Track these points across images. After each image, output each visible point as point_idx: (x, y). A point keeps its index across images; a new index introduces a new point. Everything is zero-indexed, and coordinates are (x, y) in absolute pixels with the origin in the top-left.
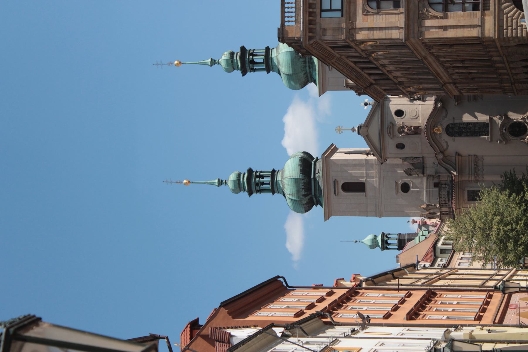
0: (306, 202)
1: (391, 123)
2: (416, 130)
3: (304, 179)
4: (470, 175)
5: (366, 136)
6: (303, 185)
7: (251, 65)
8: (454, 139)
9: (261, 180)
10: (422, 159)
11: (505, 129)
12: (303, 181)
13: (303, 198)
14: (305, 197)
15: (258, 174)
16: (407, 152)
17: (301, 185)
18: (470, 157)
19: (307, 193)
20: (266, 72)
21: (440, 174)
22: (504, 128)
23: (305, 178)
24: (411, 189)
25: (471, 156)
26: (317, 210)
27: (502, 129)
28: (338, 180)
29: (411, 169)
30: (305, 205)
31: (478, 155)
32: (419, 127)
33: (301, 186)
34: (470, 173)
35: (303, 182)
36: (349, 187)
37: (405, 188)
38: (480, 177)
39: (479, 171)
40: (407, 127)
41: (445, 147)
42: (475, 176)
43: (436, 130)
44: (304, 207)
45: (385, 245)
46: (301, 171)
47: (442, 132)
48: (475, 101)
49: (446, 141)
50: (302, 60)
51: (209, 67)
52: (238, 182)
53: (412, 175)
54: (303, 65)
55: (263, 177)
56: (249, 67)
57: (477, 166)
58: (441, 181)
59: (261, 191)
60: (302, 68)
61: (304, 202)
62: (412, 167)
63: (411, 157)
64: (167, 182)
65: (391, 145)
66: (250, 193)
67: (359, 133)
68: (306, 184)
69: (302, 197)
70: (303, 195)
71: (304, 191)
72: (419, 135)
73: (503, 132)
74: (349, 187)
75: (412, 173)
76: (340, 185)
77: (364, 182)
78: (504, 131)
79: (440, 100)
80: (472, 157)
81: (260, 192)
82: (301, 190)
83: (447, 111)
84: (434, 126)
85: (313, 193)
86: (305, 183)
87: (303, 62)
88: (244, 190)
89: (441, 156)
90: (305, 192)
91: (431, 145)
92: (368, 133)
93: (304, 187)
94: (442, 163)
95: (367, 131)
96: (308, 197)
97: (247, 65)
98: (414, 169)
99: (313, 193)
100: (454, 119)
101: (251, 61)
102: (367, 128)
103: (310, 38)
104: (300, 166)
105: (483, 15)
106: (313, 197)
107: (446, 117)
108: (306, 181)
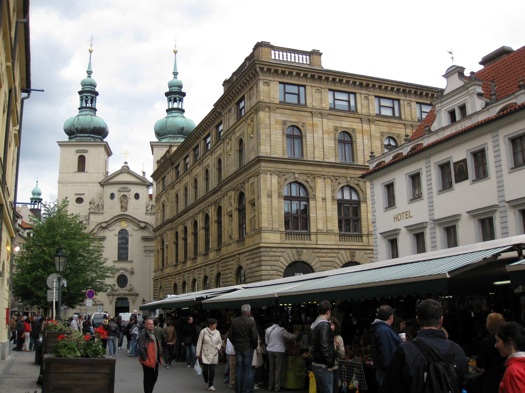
1: (130, 190)
2: (124, 207)
7: (173, 98)
9: (90, 100)
12: (88, 128)
15: (94, 99)
16: (107, 201)
17: (85, 126)
20: (167, 108)
22: (123, 271)
24: (78, 205)
26: (65, 138)
29: (94, 204)
30: (69, 129)
32: (127, 210)
36: (82, 160)
37: (79, 200)
40: (127, 201)
41: (110, 229)
44: (68, 129)
45: (34, 201)
46: (95, 127)
50: (176, 132)
51: (172, 71)
52: (90, 84)
55: (92, 103)
59: (82, 99)
61: (72, 128)
62: (96, 204)
64: (92, 37)
65: (114, 189)
66: (80, 93)
67: (123, 167)
69: (76, 126)
70: (78, 128)
71: (81, 128)
72: (120, 210)
74: (82, 160)
78: (121, 271)
79: (146, 225)
85: (78, 135)
86: (86, 129)
87: (175, 133)
88: (82, 89)
89: (104, 225)
91: (113, 218)
96: (75, 131)
97: (173, 96)
99: (78, 135)
103: (262, 69)
105: (281, 232)
106: (75, 135)
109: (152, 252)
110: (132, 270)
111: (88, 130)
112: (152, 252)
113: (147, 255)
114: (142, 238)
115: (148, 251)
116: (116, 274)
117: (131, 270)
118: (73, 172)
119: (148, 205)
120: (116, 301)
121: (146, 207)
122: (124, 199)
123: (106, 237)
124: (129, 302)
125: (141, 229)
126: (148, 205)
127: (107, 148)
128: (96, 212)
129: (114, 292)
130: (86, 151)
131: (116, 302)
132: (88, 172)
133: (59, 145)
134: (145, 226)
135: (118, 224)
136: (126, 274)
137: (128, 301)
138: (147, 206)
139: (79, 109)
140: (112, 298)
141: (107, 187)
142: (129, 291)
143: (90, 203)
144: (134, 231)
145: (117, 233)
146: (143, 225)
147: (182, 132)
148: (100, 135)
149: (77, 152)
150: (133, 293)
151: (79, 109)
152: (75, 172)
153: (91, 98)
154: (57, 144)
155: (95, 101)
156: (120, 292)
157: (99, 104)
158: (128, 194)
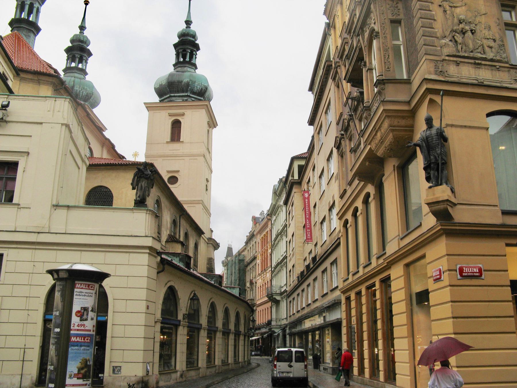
15: (194, 53)
26: (156, 99)
36: (176, 125)
74: (176, 125)
76: (180, 118)
127: (209, 111)
130: (183, 115)
132: (184, 141)
133: (146, 107)
139: (174, 65)
148: (201, 97)
149: (170, 115)
151: (174, 65)
152: (167, 142)
153: (190, 51)
154: (144, 106)
155: (195, 56)
157: (200, 58)
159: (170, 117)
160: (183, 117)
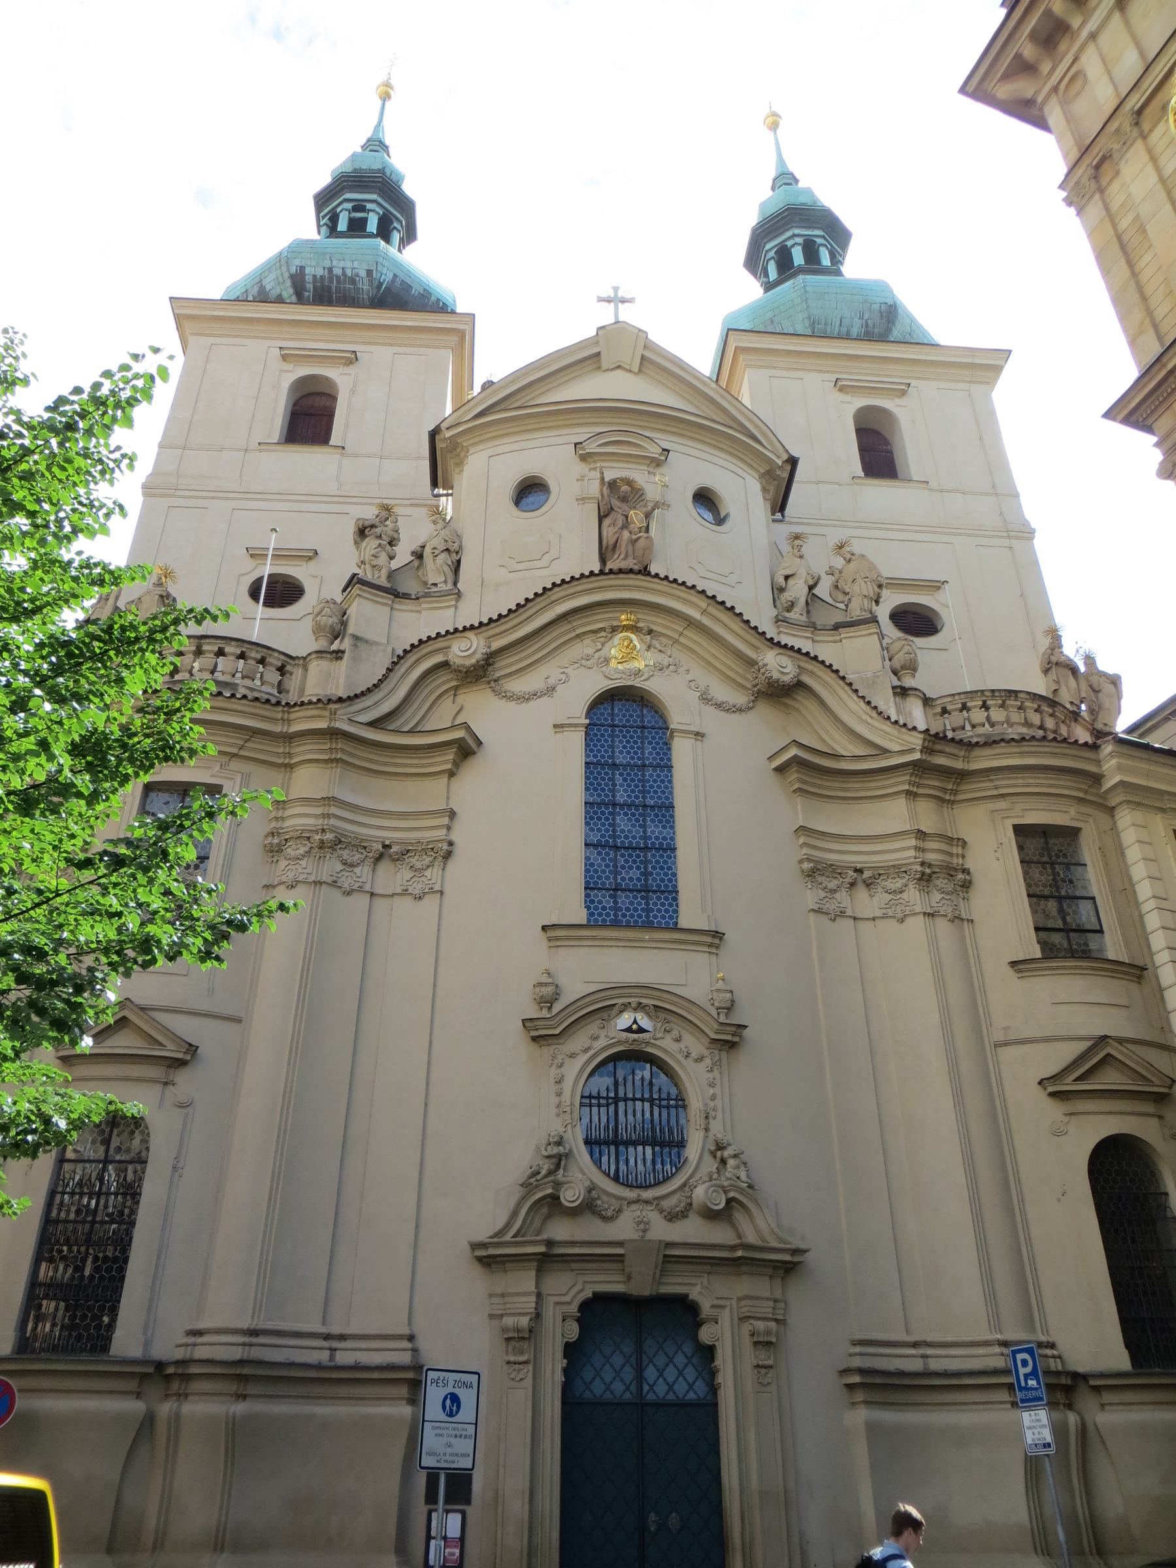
0: (268, 288)
3: (371, 282)
4: (319, 811)
5: (598, 354)
6: (344, 273)
7: (799, 240)
8: (570, 725)
10: (442, 587)
11: (641, 1030)
12: (363, 274)
13: (288, 270)
14: (292, 277)
17: (348, 264)
18: (446, 821)
19: (310, 286)
21: (346, 656)
23: (376, 284)
25: (449, 828)
27: (640, 1007)
28: (352, 366)
30: (256, 289)
31: (452, 865)
33: (342, 264)
34: (333, 810)
35: (357, 275)
38: (303, 863)
39: (339, 867)
40: (648, 516)
41: (517, 685)
42: (316, 832)
43: (631, 641)
47: (616, 671)
48: (806, 866)
49: (558, 688)
53: (356, 543)
54: (837, 328)
56: (794, 235)
57: (379, 858)
58: (306, 669)
60: (825, 324)
62: (403, 556)
63: (460, 547)
68: (347, 286)
69: (297, 262)
70: (302, 268)
71: (320, 272)
73: (621, 1012)
75: (370, 544)
77: (331, 443)
78: (625, 1020)
79: (806, 679)
80: (444, 831)
81: (328, 223)
82: (327, 264)
83: (740, 710)
84: (650, 632)
86: (353, 281)
87: (848, 333)
89: (465, 651)
90: (315, 276)
92: (608, 370)
93: (338, 277)
94: (418, 662)
95: (619, 367)
97: (797, 231)
98: (391, 558)
100: (699, 735)
101: (815, 242)
102: (636, 369)
104: (422, 292)
107: (706, 699)
108: (361, 286)
109: (868, 884)
110: (730, 1008)
111: (364, 286)
112: (868, 884)
113: (831, 906)
114: (780, 770)
115: (834, 870)
116: (579, 1041)
117: (714, 1013)
118: (253, 444)
119: (787, 578)
120: (573, 1331)
121: (778, 590)
122: (624, 499)
123: (480, 743)
124: (708, 1352)
125: (764, 709)
126: (787, 578)
128: (401, 590)
129: (561, 1230)
131: (570, 1350)
134: (799, 685)
135: (586, 647)
136: (666, 1046)
137: (706, 1334)
138: (782, 580)
140: (530, 1303)
141: (490, 452)
142: (711, 1215)
143: (362, 532)
144: (710, 710)
145: (578, 711)
146: (778, 665)
147: (888, 330)
150: (751, 1239)
156: (623, 1229)
158: (651, 478)
159: (289, 367)
160: (347, 370)
